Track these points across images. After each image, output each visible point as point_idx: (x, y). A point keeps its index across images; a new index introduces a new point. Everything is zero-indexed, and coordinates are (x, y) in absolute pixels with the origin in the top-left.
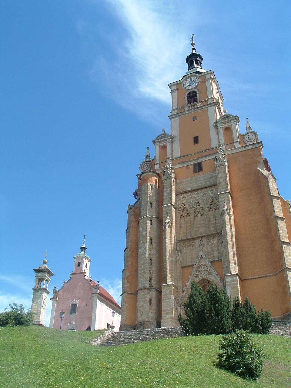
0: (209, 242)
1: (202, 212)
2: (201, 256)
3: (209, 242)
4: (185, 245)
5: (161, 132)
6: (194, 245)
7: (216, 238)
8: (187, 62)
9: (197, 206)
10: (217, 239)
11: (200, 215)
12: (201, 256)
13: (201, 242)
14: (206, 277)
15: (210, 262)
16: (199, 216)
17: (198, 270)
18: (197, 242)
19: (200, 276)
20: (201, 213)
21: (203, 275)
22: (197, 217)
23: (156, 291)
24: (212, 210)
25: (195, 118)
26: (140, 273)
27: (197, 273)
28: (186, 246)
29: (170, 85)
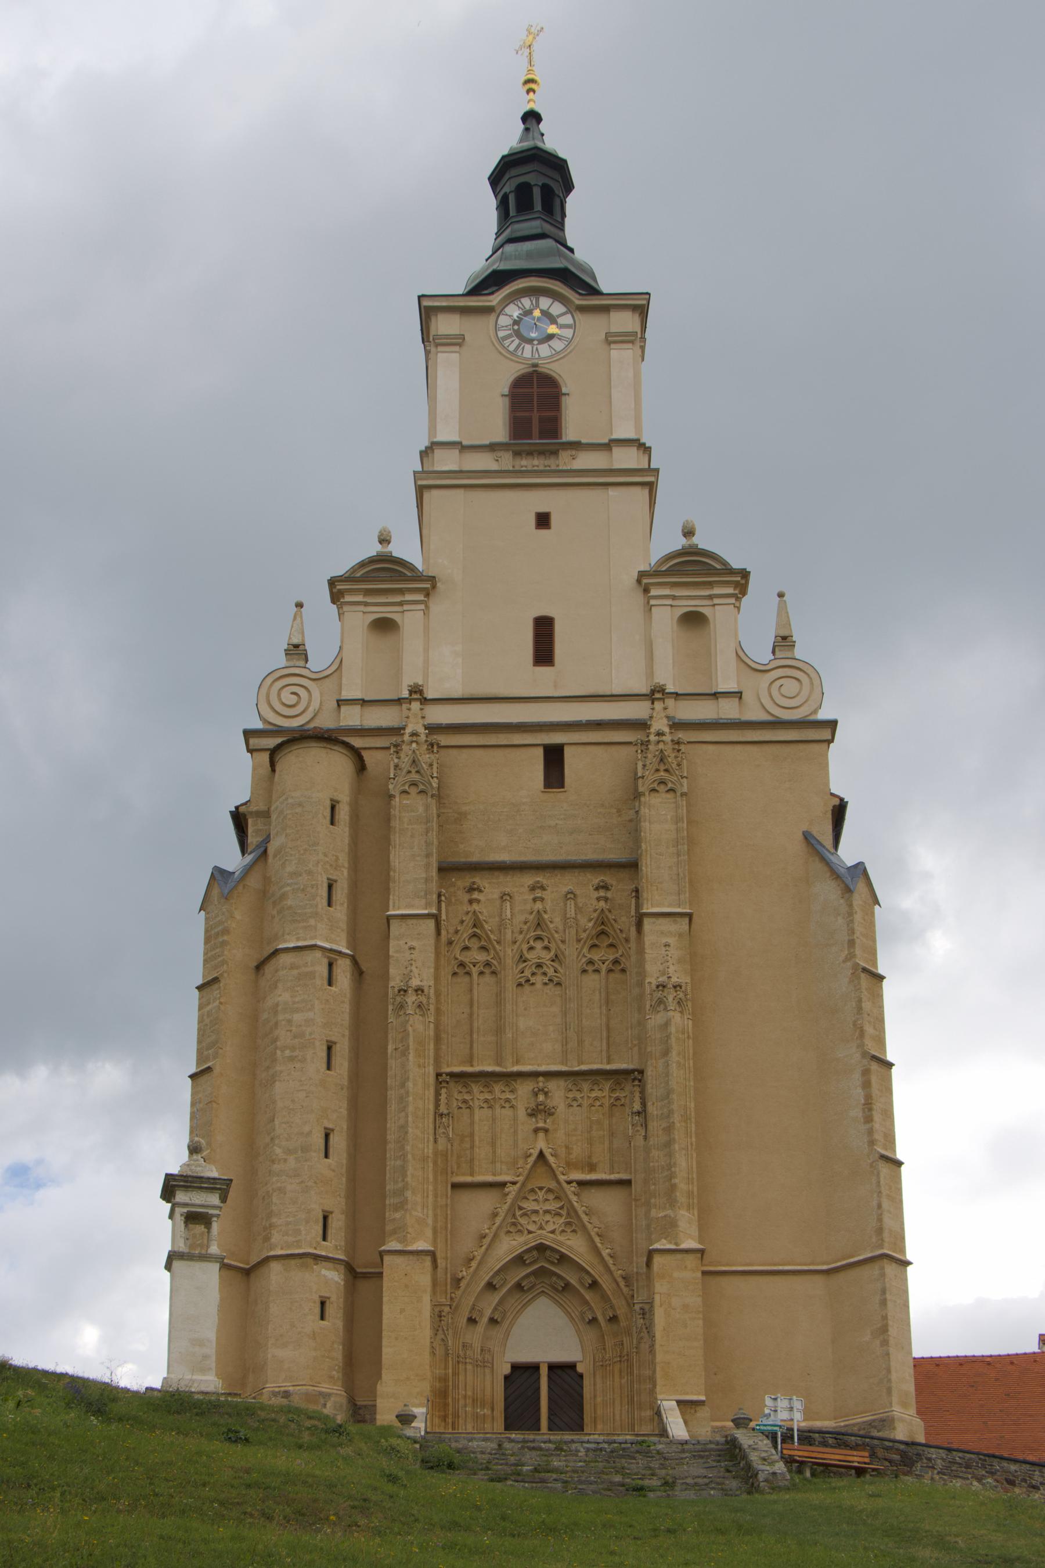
0: (575, 1099)
1: (552, 970)
2: (541, 1154)
3: (575, 1099)
4: (467, 1097)
5: (374, 549)
6: (508, 1100)
7: (606, 1093)
8: (495, 180)
9: (532, 943)
10: (610, 1097)
11: (539, 979)
12: (541, 1154)
13: (541, 1098)
14: (554, 1241)
15: (574, 1184)
16: (539, 986)
17: (520, 1208)
18: (524, 1089)
19: (530, 1232)
20: (545, 974)
21: (541, 1228)
22: (527, 988)
23: (345, 1266)
24: (597, 971)
25: (543, 521)
26: (279, 1185)
27: (514, 1216)
28: (472, 1099)
29: (426, 303)
